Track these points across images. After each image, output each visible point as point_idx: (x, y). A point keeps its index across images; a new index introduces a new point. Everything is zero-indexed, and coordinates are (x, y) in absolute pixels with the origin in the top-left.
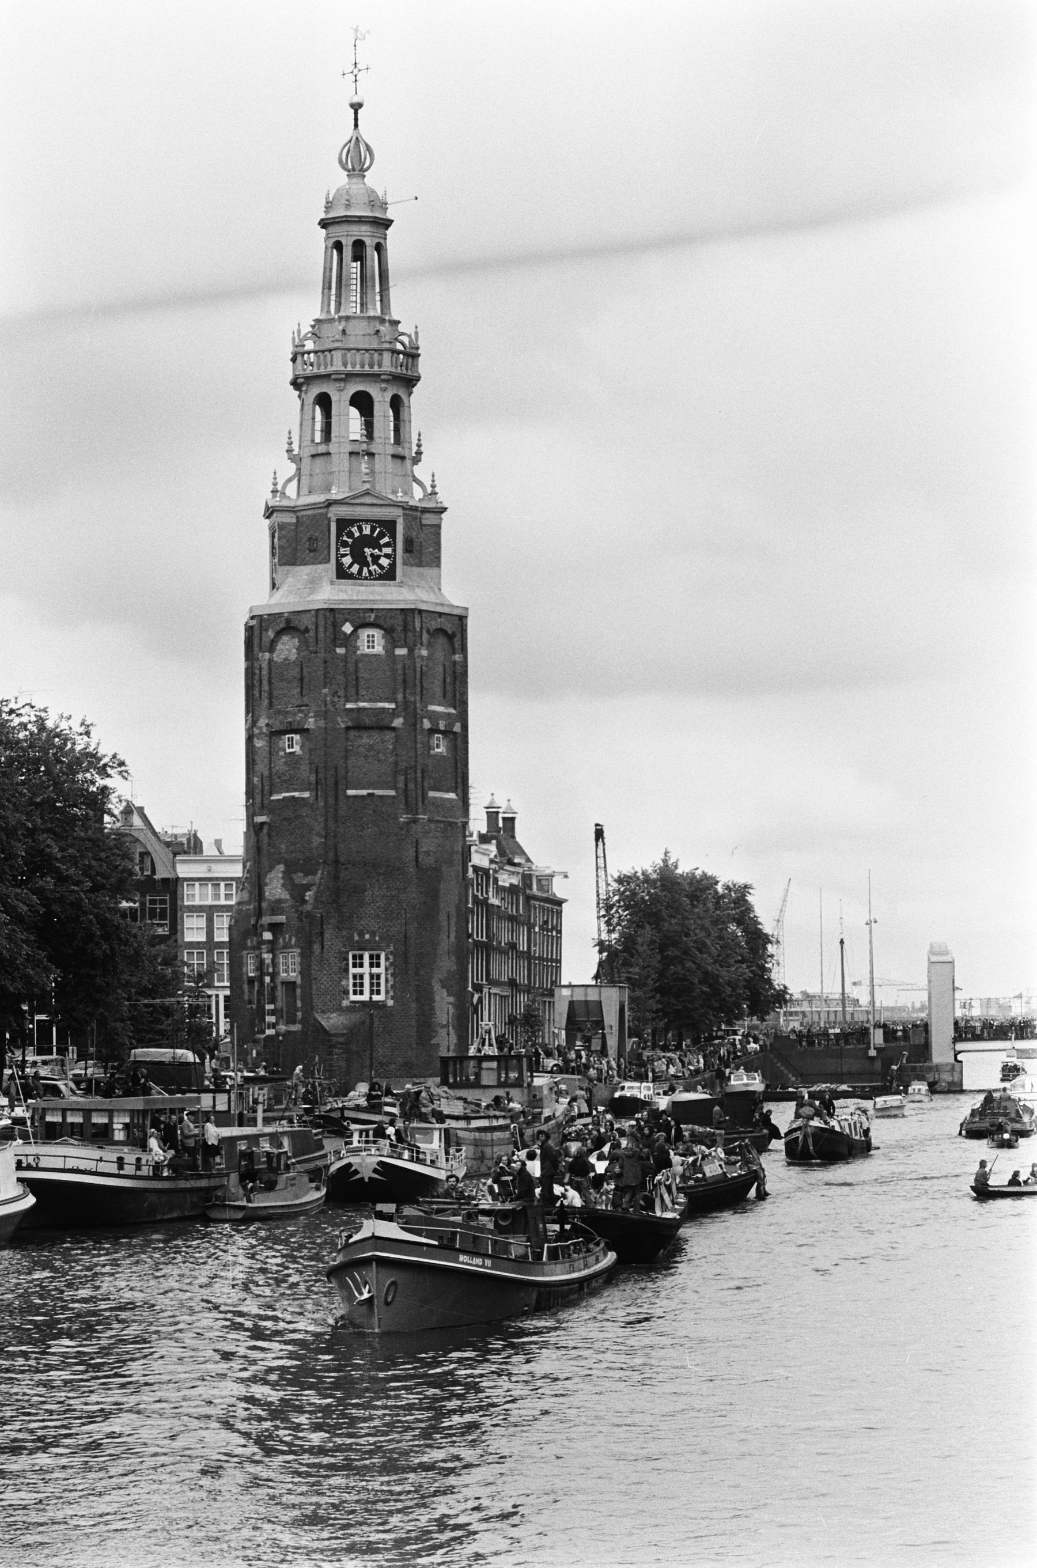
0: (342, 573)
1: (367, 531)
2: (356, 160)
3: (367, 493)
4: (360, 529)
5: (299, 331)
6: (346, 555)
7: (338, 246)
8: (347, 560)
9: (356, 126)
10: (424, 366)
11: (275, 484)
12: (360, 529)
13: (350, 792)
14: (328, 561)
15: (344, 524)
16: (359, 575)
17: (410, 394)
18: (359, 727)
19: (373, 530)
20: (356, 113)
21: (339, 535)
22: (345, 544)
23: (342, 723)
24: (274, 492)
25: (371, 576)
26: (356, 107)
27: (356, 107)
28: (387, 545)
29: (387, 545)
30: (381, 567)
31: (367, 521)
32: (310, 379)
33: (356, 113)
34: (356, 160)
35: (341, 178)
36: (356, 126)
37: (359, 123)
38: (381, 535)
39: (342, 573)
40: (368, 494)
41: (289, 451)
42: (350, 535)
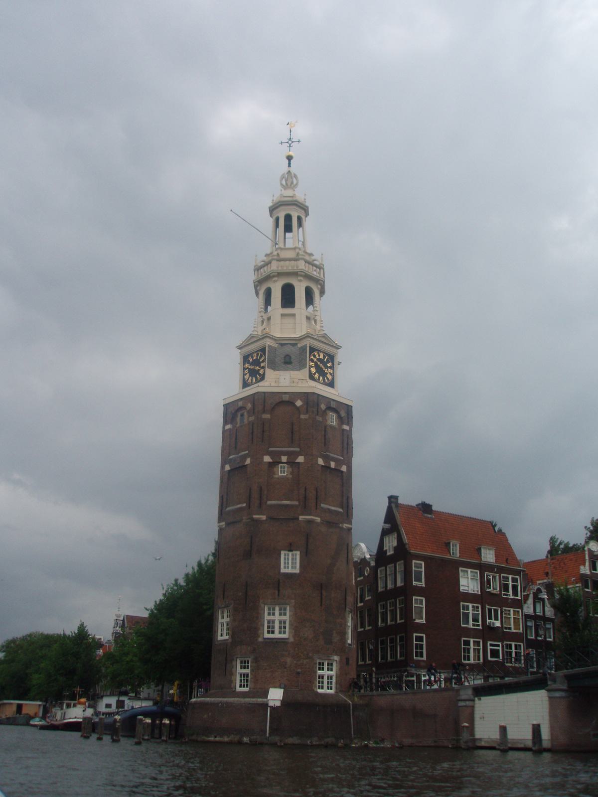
0: (311, 377)
1: (322, 357)
2: (289, 180)
3: (325, 336)
4: (319, 356)
6: (313, 367)
7: (288, 218)
8: (313, 370)
9: (289, 165)
12: (319, 356)
13: (322, 505)
14: (306, 367)
15: (312, 350)
16: (317, 381)
19: (324, 357)
21: (310, 356)
22: (312, 360)
25: (324, 383)
26: (290, 158)
27: (290, 158)
28: (330, 367)
29: (330, 367)
30: (328, 379)
31: (323, 352)
32: (280, 274)
34: (289, 180)
36: (289, 165)
37: (291, 165)
38: (328, 361)
39: (311, 377)
40: (323, 337)
42: (315, 356)
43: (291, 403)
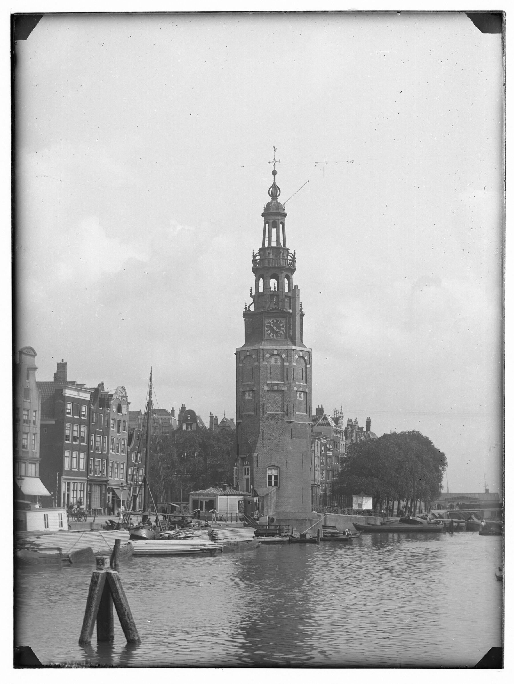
2: (274, 191)
5: (254, 253)
9: (274, 180)
10: (297, 265)
11: (246, 306)
17: (292, 274)
18: (271, 390)
20: (274, 177)
23: (266, 388)
24: (246, 308)
26: (274, 173)
27: (274, 173)
33: (274, 177)
34: (274, 191)
35: (269, 199)
36: (274, 180)
41: (251, 294)
43: (250, 356)
